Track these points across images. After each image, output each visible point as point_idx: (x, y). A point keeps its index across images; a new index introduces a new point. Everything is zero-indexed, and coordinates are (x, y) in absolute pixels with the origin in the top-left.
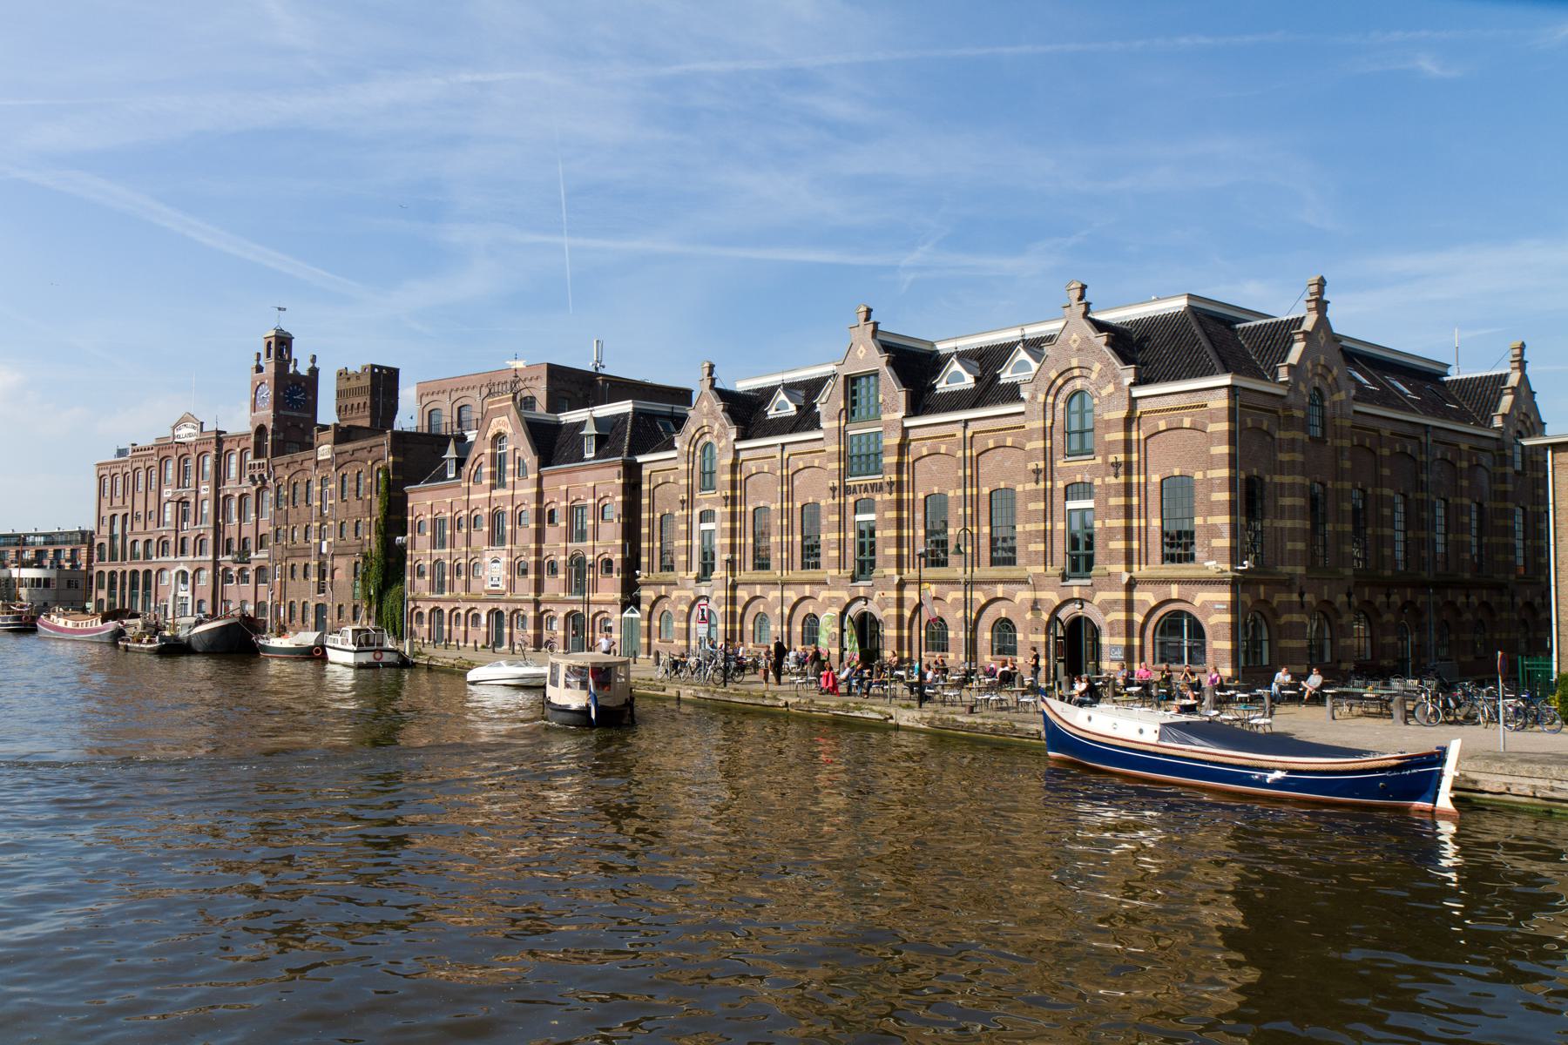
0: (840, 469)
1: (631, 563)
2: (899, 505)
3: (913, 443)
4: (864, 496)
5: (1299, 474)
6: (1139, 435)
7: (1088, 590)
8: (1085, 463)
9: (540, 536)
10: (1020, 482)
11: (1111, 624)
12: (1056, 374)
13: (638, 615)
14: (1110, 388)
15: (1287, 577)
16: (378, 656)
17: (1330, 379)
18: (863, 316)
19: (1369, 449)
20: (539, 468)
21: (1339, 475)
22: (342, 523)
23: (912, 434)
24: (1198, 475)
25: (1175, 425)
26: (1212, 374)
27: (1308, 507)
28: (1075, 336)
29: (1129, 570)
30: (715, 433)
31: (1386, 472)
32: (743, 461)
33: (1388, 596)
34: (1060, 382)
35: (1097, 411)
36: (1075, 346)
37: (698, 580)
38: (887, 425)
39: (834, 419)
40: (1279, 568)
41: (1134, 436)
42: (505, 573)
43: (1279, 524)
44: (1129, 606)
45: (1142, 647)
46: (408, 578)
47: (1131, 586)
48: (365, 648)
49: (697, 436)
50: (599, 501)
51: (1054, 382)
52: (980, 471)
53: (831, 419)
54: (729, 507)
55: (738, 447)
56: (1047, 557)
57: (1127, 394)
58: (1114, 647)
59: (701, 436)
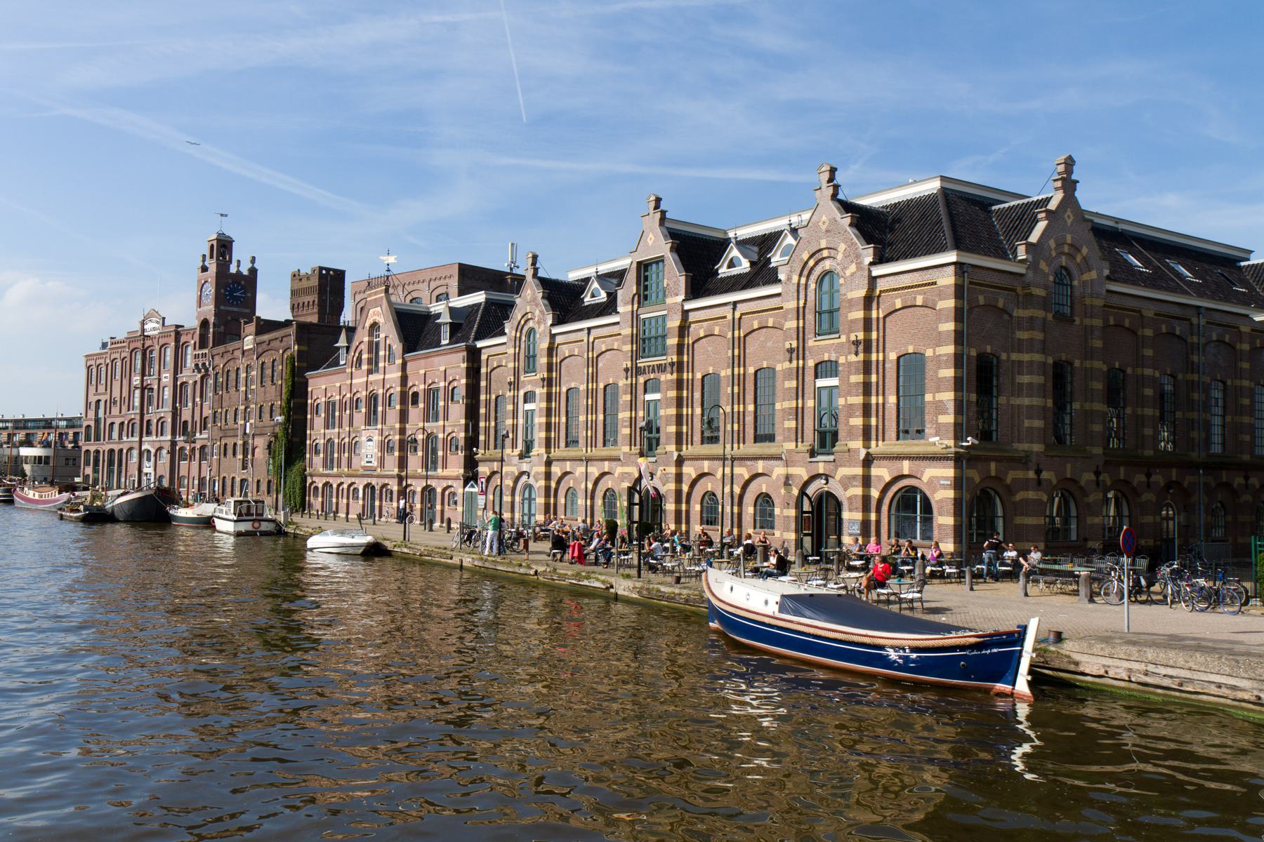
0: (632, 351)
1: (472, 442)
2: (679, 384)
3: (692, 325)
4: (652, 376)
5: (1038, 352)
6: (878, 313)
7: (831, 466)
8: (832, 341)
9: (404, 417)
10: (779, 362)
11: (850, 499)
12: (808, 256)
13: (476, 490)
15: (1022, 454)
16: (256, 525)
17: (1079, 258)
18: (653, 205)
19: (1128, 329)
20: (403, 355)
21: (1088, 354)
22: (261, 406)
23: (692, 317)
24: (929, 353)
25: (909, 304)
26: (944, 251)
27: (1050, 385)
28: (824, 218)
29: (867, 446)
31: (1149, 352)
32: (558, 345)
33: (1148, 475)
34: (811, 263)
35: (843, 291)
36: (824, 228)
37: (521, 456)
40: (1016, 445)
41: (874, 314)
42: (376, 450)
43: (1016, 401)
44: (866, 481)
45: (878, 522)
46: (308, 456)
48: (245, 518)
49: (523, 322)
50: (449, 384)
51: (806, 263)
52: (747, 351)
53: (626, 304)
54: (545, 388)
55: (554, 331)
56: (798, 434)
57: (866, 273)
58: (852, 521)
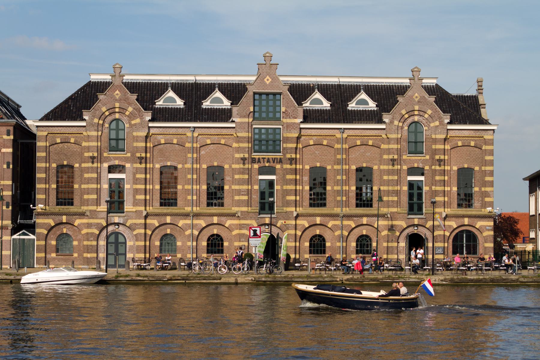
4: (267, 165)
7: (423, 221)
8: (420, 158)
10: (376, 165)
12: (406, 112)
14: (437, 123)
24: (477, 168)
25: (466, 144)
28: (416, 95)
30: (127, 113)
36: (417, 100)
37: (109, 212)
38: (289, 126)
39: (245, 117)
47: (146, 217)
49: (107, 113)
59: (110, 114)
